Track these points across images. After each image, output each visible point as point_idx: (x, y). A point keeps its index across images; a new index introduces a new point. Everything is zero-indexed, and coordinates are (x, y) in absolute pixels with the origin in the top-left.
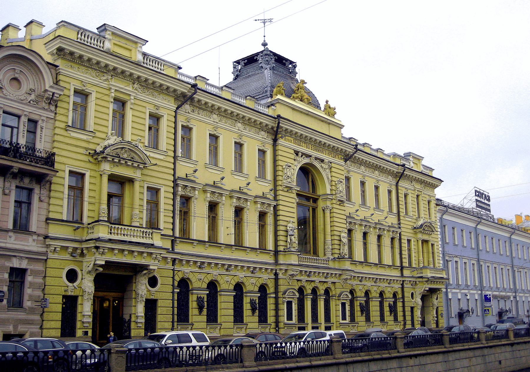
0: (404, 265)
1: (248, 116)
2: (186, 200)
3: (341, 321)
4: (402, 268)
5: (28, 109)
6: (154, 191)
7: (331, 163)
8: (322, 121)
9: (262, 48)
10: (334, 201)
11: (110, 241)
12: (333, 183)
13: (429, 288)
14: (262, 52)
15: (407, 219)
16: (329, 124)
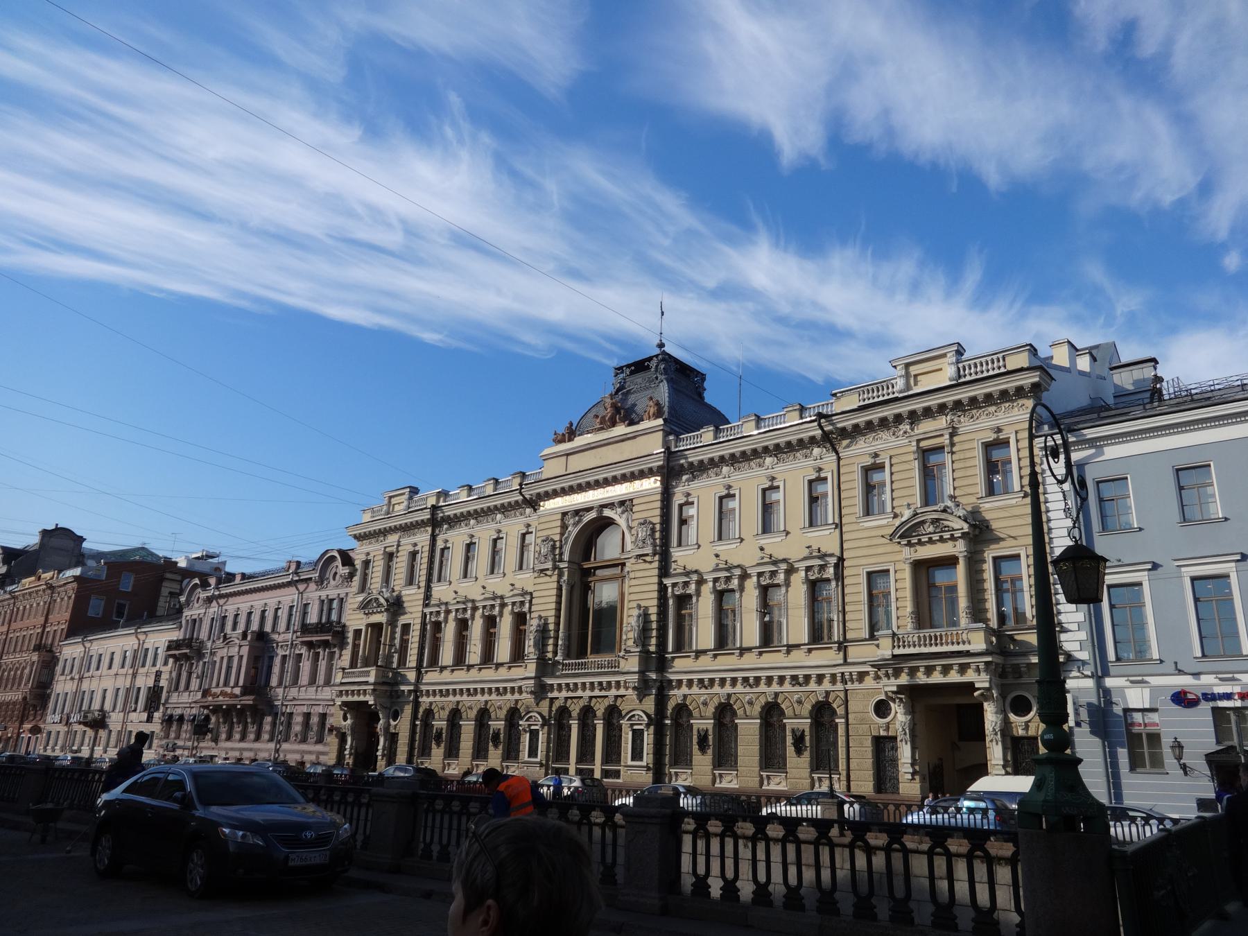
0: (849, 636)
1: (498, 503)
2: (437, 627)
3: (630, 763)
4: (842, 646)
5: (338, 591)
6: (406, 628)
7: (631, 500)
8: (623, 441)
9: (657, 351)
10: (633, 560)
11: (342, 684)
12: (634, 532)
13: (898, 686)
14: (657, 356)
15: (867, 525)
16: (634, 437)
